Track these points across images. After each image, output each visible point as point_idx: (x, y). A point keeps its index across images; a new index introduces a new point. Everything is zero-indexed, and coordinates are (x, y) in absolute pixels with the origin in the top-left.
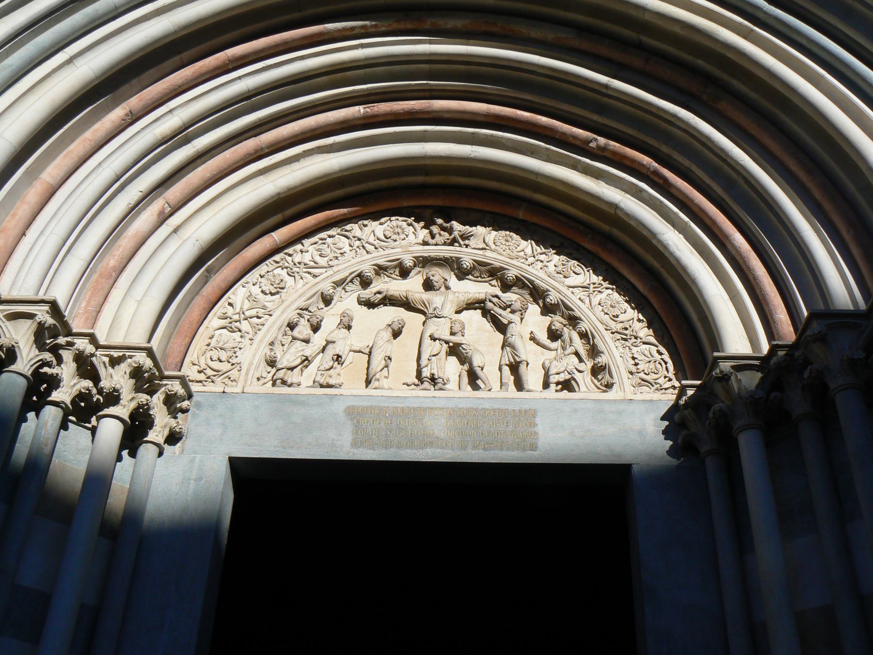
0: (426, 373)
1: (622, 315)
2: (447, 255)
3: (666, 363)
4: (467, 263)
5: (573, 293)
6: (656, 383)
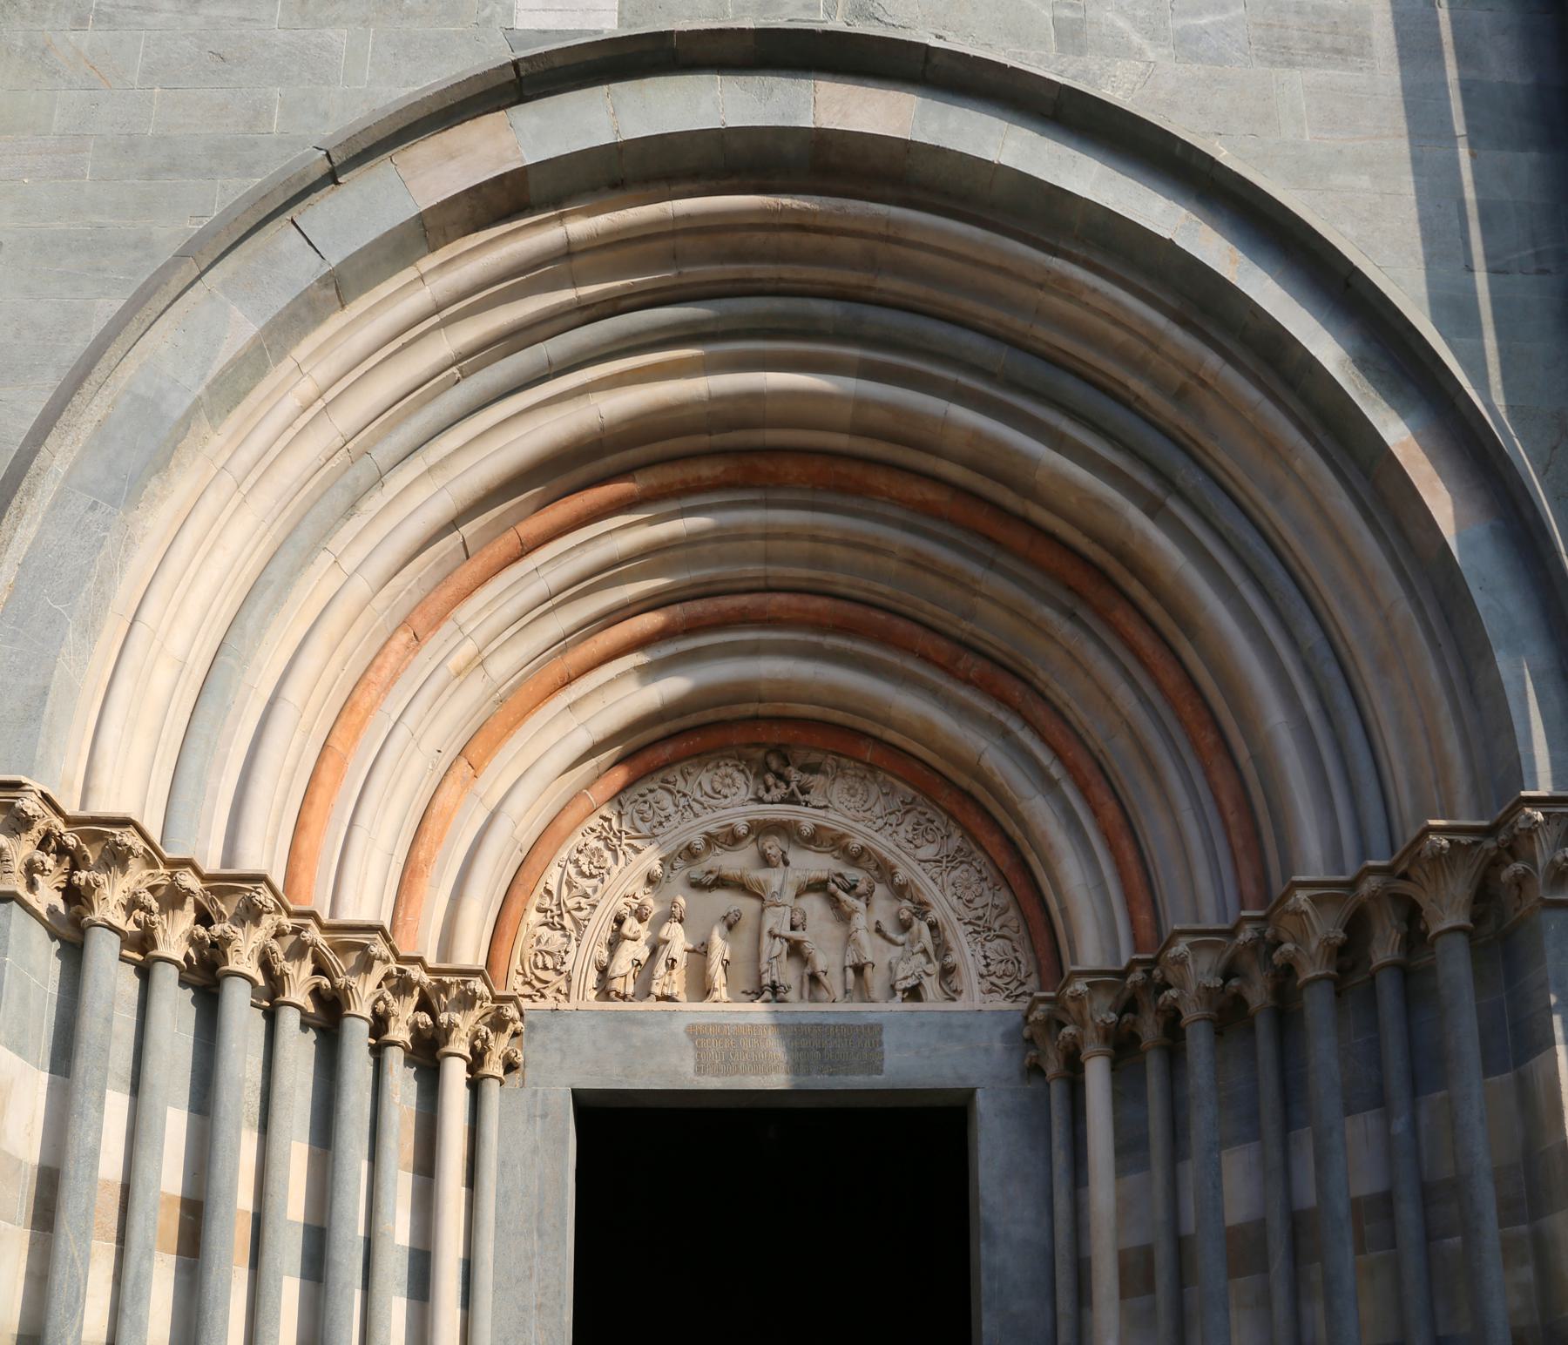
0: (766, 980)
1: (977, 898)
2: (785, 818)
3: (1019, 962)
4: (807, 827)
5: (924, 870)
6: (1007, 989)
